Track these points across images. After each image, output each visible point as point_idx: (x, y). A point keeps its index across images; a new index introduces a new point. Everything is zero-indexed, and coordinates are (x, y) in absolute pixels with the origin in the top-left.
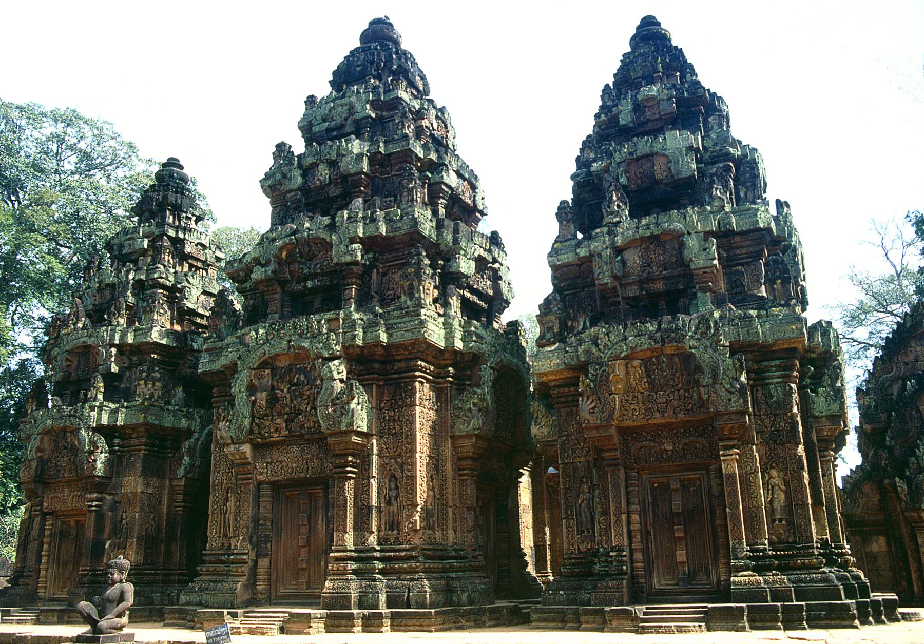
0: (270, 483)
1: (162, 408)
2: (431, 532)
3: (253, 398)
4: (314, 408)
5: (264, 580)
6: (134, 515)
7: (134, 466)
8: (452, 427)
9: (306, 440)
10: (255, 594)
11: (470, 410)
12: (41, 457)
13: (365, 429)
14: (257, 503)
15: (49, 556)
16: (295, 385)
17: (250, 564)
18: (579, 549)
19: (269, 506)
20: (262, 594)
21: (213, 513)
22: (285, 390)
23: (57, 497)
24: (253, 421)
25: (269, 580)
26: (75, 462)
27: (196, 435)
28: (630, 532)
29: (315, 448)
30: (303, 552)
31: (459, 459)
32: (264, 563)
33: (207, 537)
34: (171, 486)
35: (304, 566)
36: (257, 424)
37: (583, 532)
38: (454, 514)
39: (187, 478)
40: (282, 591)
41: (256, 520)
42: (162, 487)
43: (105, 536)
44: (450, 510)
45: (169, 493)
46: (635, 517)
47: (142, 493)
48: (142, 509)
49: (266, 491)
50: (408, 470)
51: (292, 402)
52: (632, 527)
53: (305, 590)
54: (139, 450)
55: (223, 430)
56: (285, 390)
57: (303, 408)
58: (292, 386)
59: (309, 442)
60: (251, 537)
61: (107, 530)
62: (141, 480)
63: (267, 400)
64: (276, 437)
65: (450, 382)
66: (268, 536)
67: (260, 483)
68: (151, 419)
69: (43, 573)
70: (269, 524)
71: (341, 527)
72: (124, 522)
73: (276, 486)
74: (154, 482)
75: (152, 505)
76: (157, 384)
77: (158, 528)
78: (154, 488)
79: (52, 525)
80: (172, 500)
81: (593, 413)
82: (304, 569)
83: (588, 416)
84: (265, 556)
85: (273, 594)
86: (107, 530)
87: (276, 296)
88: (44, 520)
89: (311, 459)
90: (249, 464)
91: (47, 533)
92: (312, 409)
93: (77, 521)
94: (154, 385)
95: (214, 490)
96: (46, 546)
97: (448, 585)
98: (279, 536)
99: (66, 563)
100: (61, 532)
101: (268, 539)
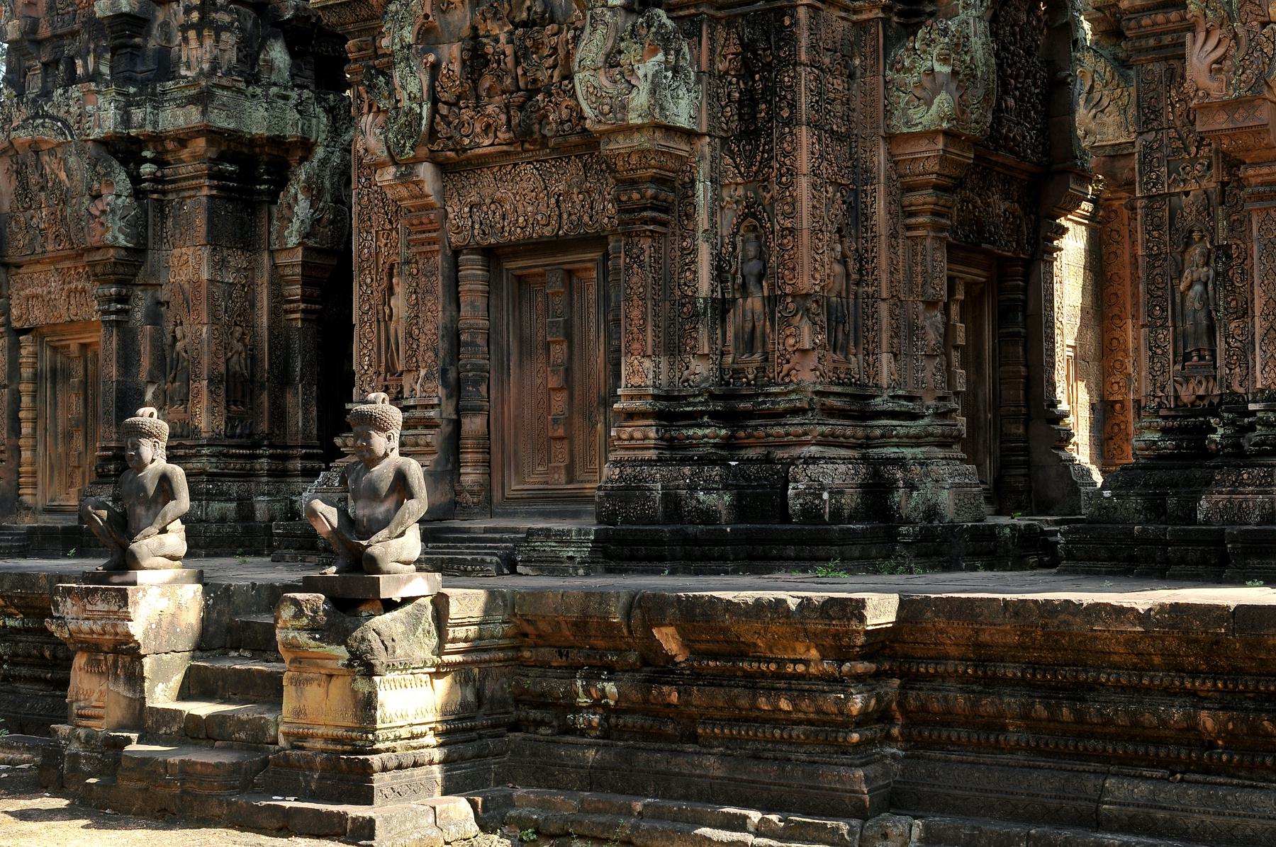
1: (239, 91)
2: (839, 357)
3: (432, 58)
4: (568, 76)
5: (476, 464)
6: (196, 332)
7: (190, 224)
8: (888, 113)
10: (457, 494)
13: (683, 122)
14: (454, 297)
15: (34, 421)
16: (524, 24)
17: (446, 429)
18: (1177, 397)
19: (481, 302)
20: (472, 493)
21: (362, 322)
22: (503, 38)
23: (36, 296)
24: (434, 111)
25: (488, 464)
26: (64, 218)
27: (320, 152)
29: (573, 169)
30: (559, 401)
31: (910, 189)
32: (473, 425)
33: (353, 374)
34: (275, 267)
35: (560, 432)
36: (443, 117)
37: (1187, 357)
38: (892, 315)
39: (307, 250)
40: (515, 486)
42: (252, 268)
43: (143, 375)
44: (884, 309)
45: (272, 283)
47: (211, 281)
48: (214, 318)
49: (472, 269)
50: (786, 216)
51: (517, 63)
53: (559, 480)
54: (200, 188)
55: (370, 136)
56: (503, 38)
57: (543, 76)
58: (516, 26)
59: (563, 153)
60: (444, 372)
61: (146, 362)
62: (205, 253)
63: (463, 62)
66: (481, 368)
67: (457, 252)
68: (220, 120)
69: (26, 455)
70: (480, 340)
71: (636, 345)
72: (179, 345)
73: (492, 255)
74: (237, 260)
75: (233, 310)
76: (225, 36)
77: (253, 359)
78: (238, 270)
79: (35, 355)
80: (278, 298)
81: (1220, 70)
82: (561, 439)
83: (1204, 80)
84: (477, 410)
85: (497, 495)
86: (146, 362)
89: (568, 193)
90: (429, 207)
91: (26, 372)
92: (564, 78)
93: (84, 346)
94: (217, 40)
95: (362, 270)
96: (26, 400)
97: (876, 474)
98: (504, 369)
99: (68, 436)
100: (54, 370)
101: (482, 376)
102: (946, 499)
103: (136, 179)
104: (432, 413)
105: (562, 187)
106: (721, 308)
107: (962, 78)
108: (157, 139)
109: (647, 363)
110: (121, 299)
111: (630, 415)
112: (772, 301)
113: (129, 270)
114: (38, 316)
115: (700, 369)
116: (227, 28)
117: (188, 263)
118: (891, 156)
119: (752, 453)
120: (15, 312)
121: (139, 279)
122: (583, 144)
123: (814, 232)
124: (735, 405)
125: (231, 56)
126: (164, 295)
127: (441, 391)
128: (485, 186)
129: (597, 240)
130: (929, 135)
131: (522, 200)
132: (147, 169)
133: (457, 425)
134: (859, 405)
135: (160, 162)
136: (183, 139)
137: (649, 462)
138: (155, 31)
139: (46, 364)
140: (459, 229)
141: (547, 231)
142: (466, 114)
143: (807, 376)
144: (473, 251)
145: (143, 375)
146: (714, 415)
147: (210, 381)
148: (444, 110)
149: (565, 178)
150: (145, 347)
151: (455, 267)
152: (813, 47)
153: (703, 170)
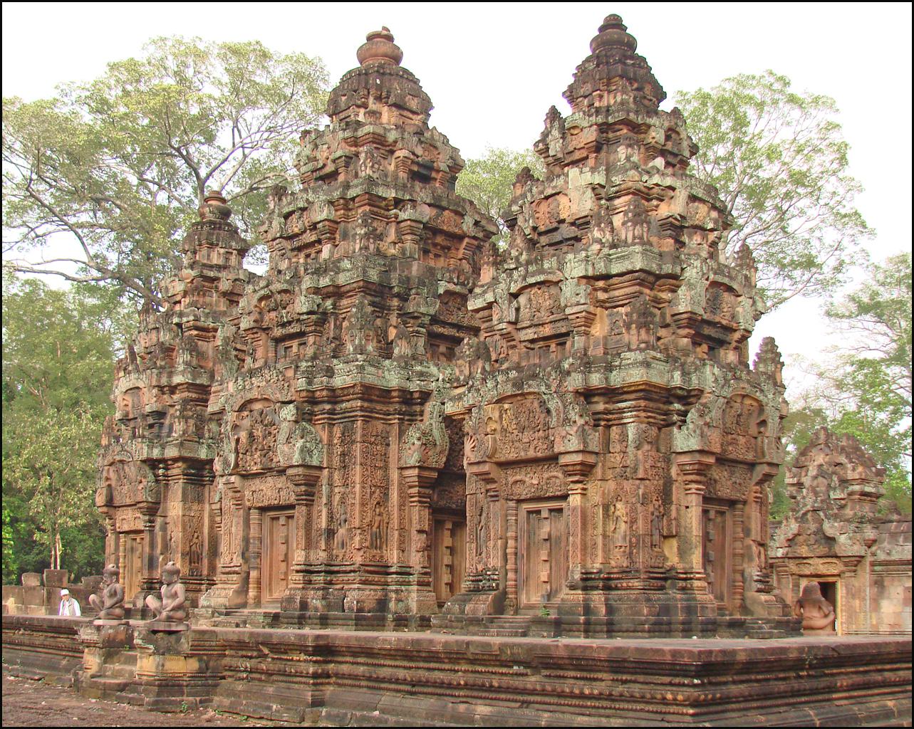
0: (256, 508)
6: (177, 534)
8: (399, 459)
9: (277, 471)
11: (414, 444)
12: (109, 486)
13: (315, 462)
16: (266, 426)
17: (244, 575)
28: (505, 555)
31: (411, 487)
32: (254, 574)
38: (400, 535)
41: (246, 540)
46: (511, 543)
49: (254, 515)
52: (508, 551)
60: (243, 554)
62: (181, 504)
64: (255, 469)
65: (399, 419)
73: (263, 510)
74: (195, 507)
87: (261, 342)
88: (118, 539)
91: (121, 548)
96: (121, 560)
100: (132, 548)
102: (414, 606)
103: (156, 476)
104: (237, 569)
105: (280, 486)
106: (331, 533)
107: (427, 444)
108: (164, 461)
109: (303, 552)
110: (150, 521)
111: (298, 571)
112: (350, 530)
113: (153, 510)
114: (126, 528)
115: (322, 555)
116: (191, 417)
117: (175, 508)
118: (401, 476)
119: (338, 586)
120: (118, 525)
121: (159, 514)
122: (282, 472)
123: (363, 505)
124: (330, 570)
125: (192, 429)
126: (168, 520)
127: (241, 561)
128: (256, 484)
129: (292, 507)
130: (415, 467)
131: (269, 490)
132: (161, 472)
133: (249, 573)
134: (384, 570)
135: (167, 469)
136: (175, 460)
137: (299, 589)
138: (169, 417)
139: (128, 546)
140: (249, 500)
141: (276, 502)
142: (249, 458)
143: (358, 559)
144: (256, 508)
145: (159, 551)
146: (326, 572)
147: (182, 554)
148: (241, 456)
149: (281, 482)
150: (159, 540)
151: (248, 514)
152: (363, 435)
153: (325, 481)
